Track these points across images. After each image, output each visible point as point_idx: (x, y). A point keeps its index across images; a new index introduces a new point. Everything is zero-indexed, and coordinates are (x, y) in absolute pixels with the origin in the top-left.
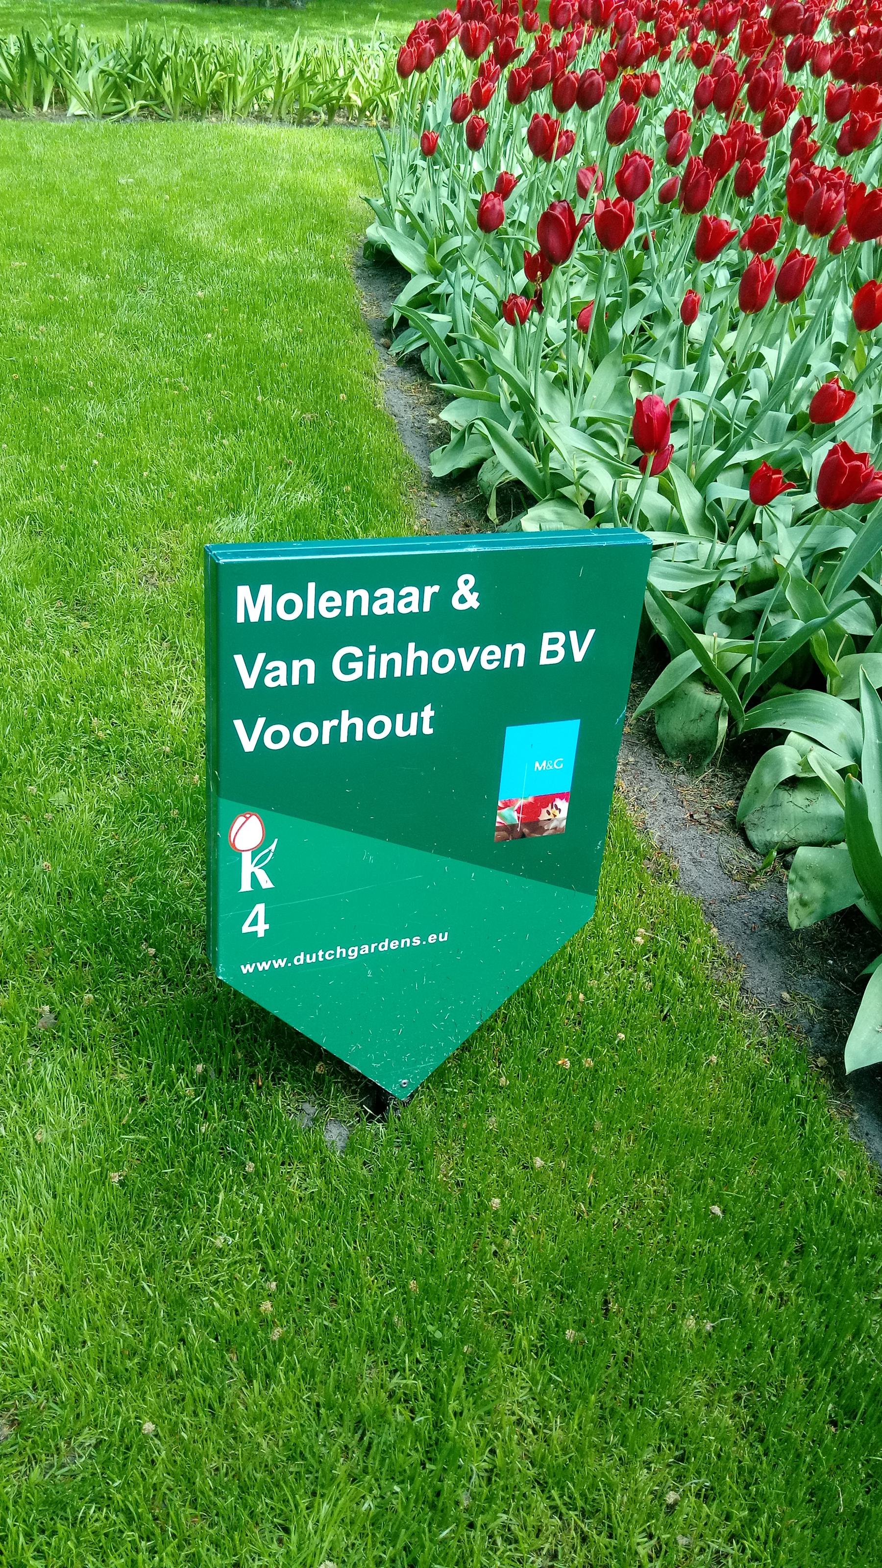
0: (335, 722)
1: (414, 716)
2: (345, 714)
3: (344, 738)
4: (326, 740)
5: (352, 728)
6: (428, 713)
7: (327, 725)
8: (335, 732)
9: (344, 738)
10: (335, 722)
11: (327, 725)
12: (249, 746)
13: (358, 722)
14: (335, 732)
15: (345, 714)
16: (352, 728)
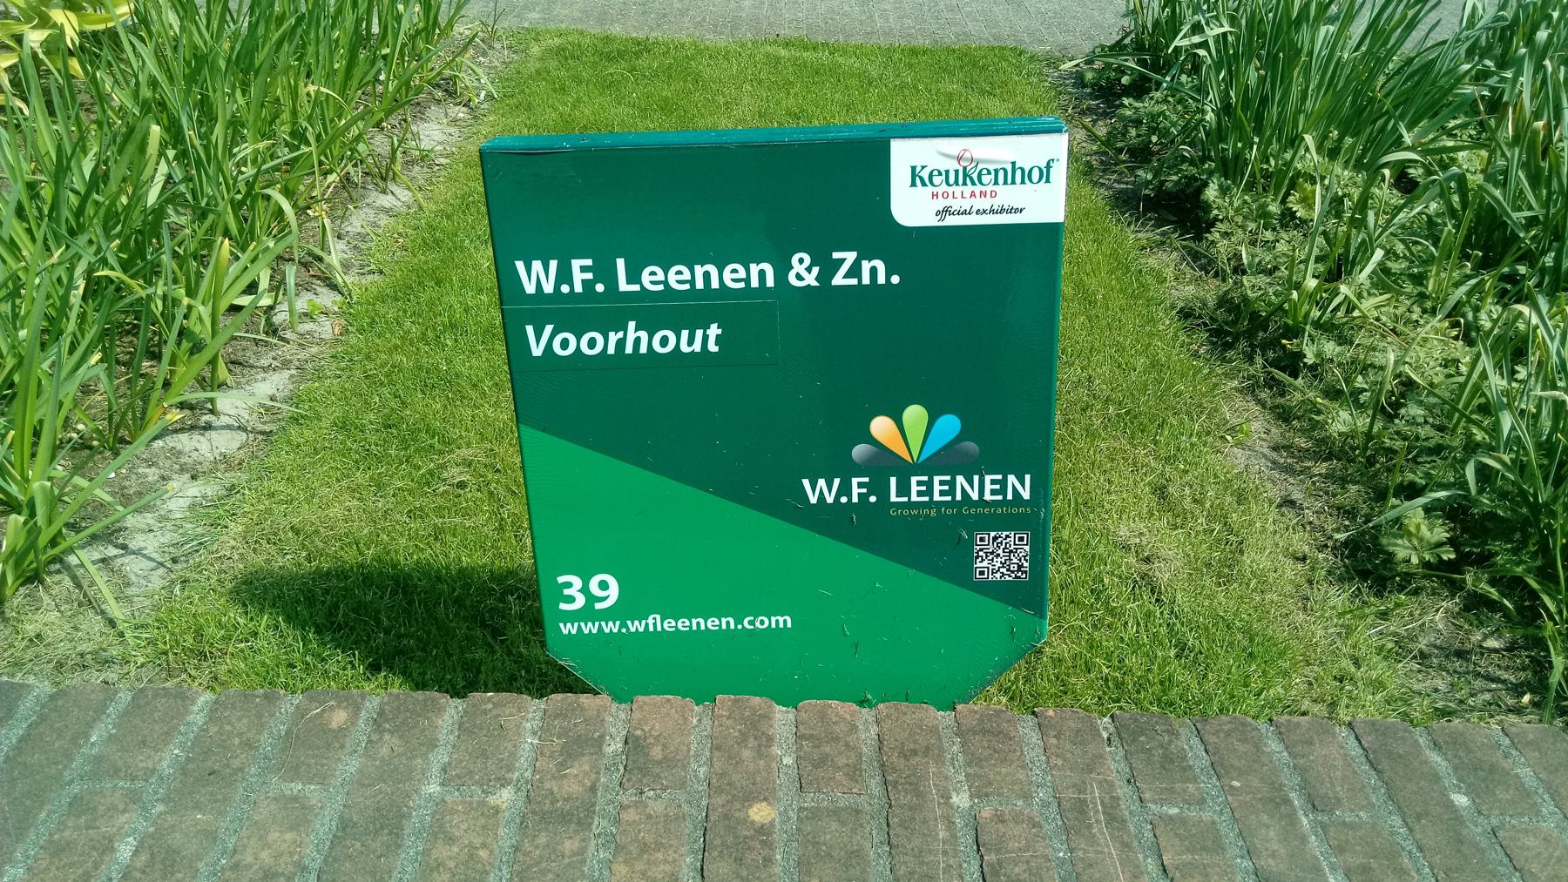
0: (620, 335)
1: (699, 333)
2: (632, 325)
3: (629, 350)
4: (611, 350)
5: (637, 341)
6: (714, 331)
7: (614, 337)
8: (621, 344)
9: (629, 350)
10: (620, 335)
11: (614, 337)
12: (537, 351)
13: (644, 335)
14: (621, 344)
15: (632, 325)
16: (637, 341)
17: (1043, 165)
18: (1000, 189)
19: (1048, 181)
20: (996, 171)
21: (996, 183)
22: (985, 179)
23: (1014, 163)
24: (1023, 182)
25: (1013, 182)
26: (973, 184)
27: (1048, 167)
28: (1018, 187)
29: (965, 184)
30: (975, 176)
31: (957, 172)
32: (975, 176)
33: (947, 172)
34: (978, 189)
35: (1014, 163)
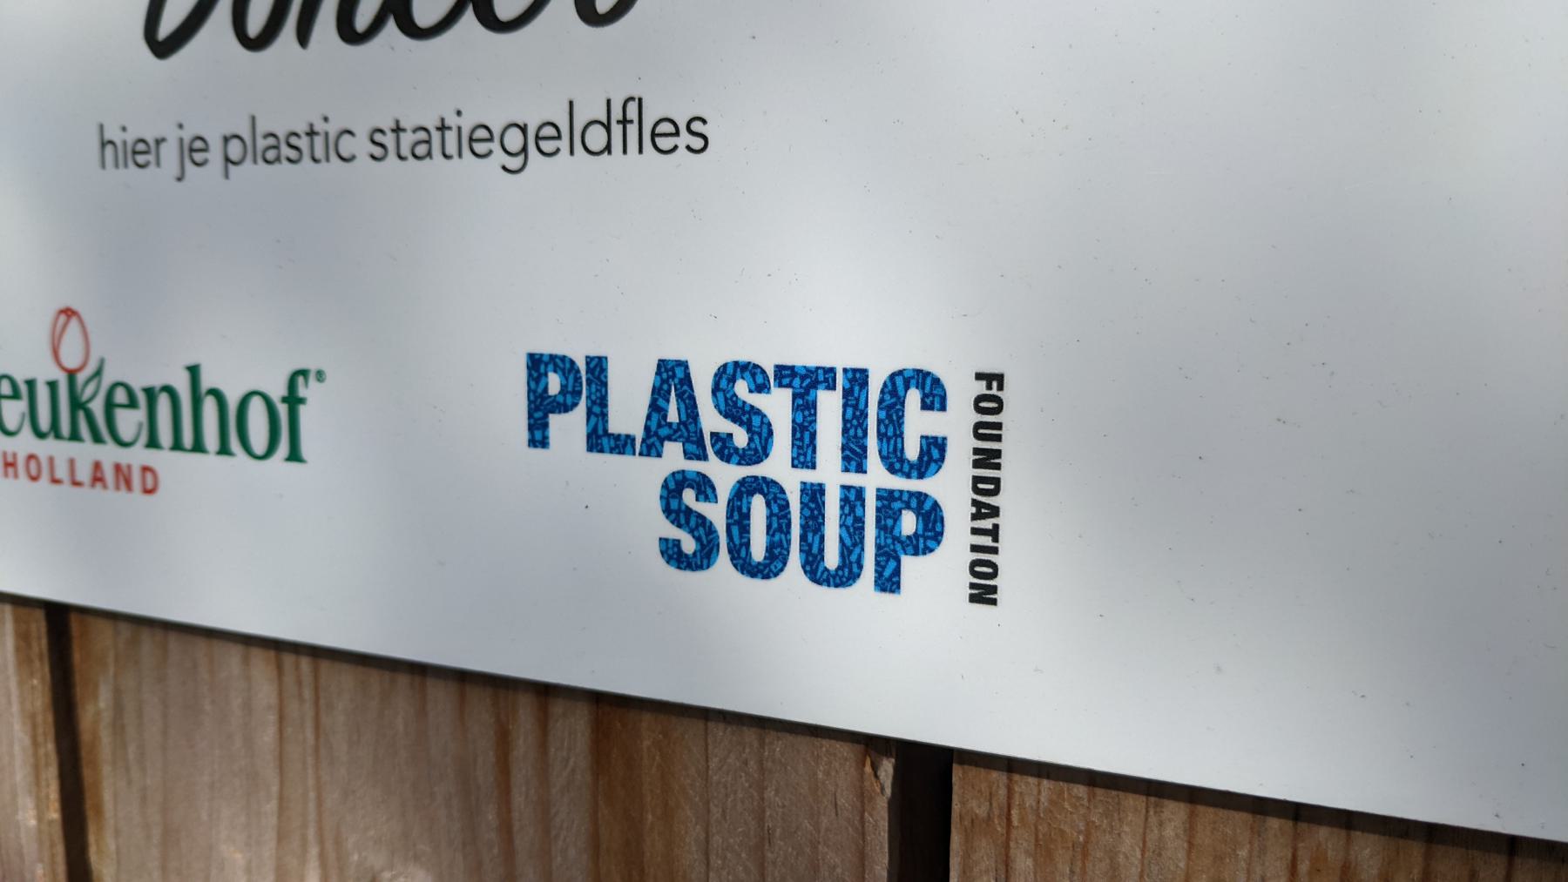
17: (277, 391)
18: (164, 461)
19: (295, 456)
20: (150, 393)
21: (153, 443)
22: (129, 422)
23: (194, 371)
24: (224, 450)
25: (198, 447)
26: (97, 439)
27: (293, 400)
28: (210, 461)
29: (75, 436)
30: (97, 407)
31: (52, 386)
32: (97, 407)
33: (31, 384)
34: (109, 454)
35: (194, 371)
